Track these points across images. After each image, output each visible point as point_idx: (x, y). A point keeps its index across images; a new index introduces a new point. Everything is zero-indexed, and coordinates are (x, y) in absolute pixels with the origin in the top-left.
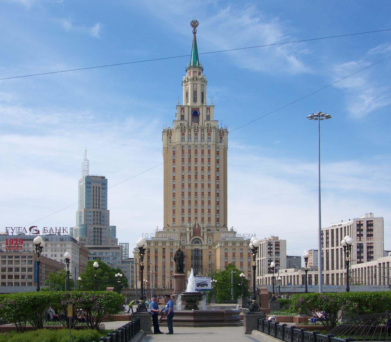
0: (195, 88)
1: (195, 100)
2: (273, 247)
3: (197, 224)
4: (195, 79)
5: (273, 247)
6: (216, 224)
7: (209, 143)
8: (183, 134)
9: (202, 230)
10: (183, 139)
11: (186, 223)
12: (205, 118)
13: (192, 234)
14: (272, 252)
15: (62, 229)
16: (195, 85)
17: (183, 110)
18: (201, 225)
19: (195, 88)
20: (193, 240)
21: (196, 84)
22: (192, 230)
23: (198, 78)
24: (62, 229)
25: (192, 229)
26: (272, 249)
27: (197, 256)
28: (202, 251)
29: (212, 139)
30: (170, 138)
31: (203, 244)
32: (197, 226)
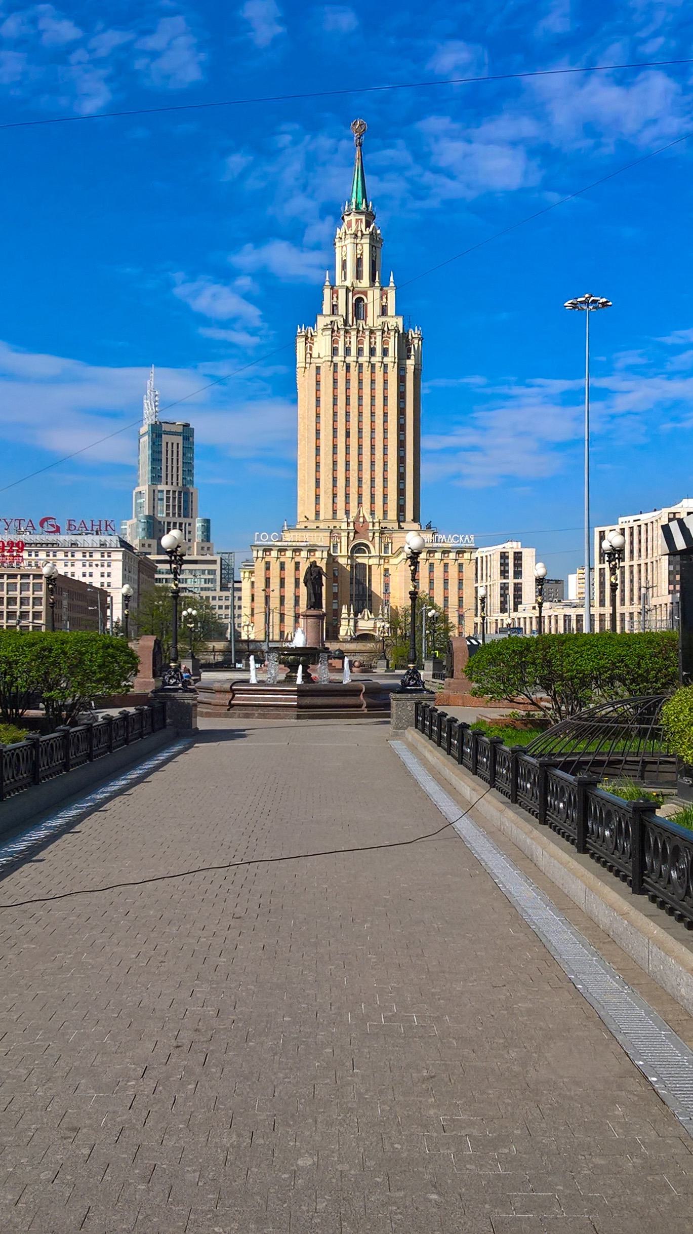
0: (359, 252)
1: (359, 276)
2: (511, 561)
3: (361, 515)
4: (359, 234)
5: (511, 561)
6: (398, 515)
7: (386, 359)
8: (334, 342)
9: (371, 528)
10: (335, 351)
11: (341, 514)
12: (378, 311)
13: (352, 534)
14: (507, 572)
15: (103, 524)
16: (359, 247)
17: (335, 296)
18: (369, 518)
19: (359, 252)
20: (355, 546)
21: (362, 244)
22: (351, 527)
23: (364, 232)
24: (103, 524)
25: (352, 524)
26: (507, 565)
27: (360, 574)
28: (370, 567)
29: (391, 352)
30: (311, 349)
31: (373, 554)
32: (361, 520)
